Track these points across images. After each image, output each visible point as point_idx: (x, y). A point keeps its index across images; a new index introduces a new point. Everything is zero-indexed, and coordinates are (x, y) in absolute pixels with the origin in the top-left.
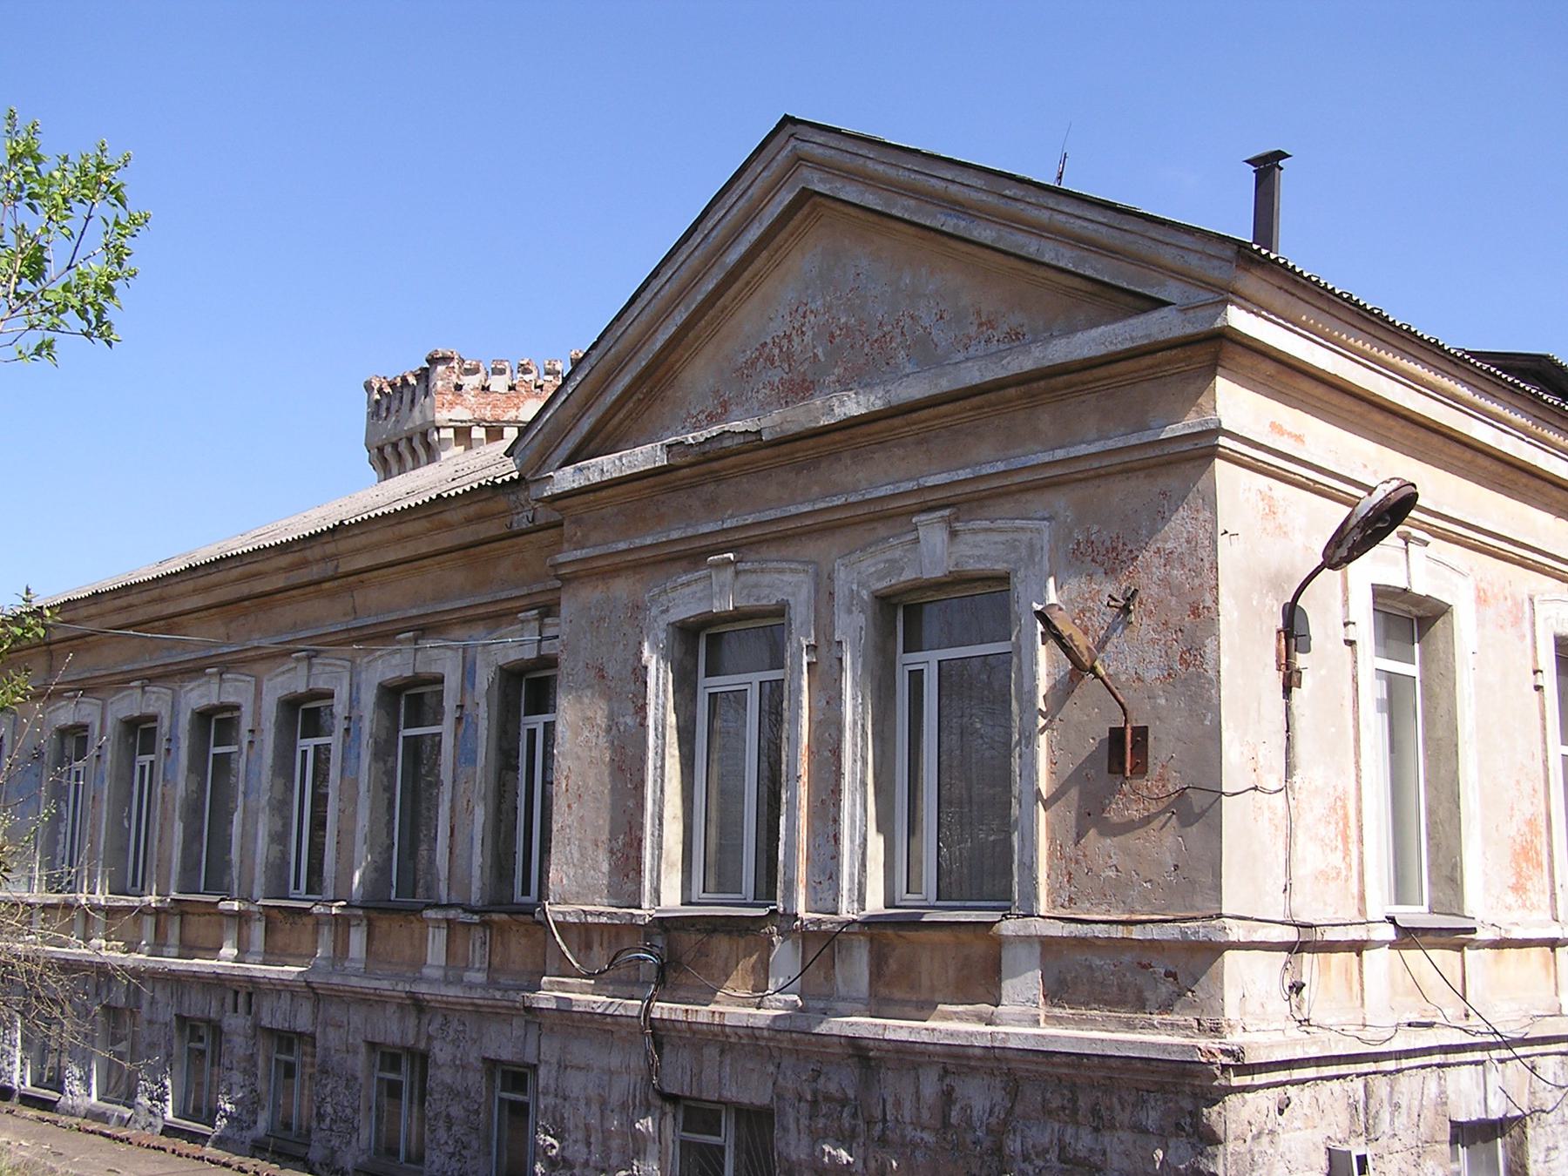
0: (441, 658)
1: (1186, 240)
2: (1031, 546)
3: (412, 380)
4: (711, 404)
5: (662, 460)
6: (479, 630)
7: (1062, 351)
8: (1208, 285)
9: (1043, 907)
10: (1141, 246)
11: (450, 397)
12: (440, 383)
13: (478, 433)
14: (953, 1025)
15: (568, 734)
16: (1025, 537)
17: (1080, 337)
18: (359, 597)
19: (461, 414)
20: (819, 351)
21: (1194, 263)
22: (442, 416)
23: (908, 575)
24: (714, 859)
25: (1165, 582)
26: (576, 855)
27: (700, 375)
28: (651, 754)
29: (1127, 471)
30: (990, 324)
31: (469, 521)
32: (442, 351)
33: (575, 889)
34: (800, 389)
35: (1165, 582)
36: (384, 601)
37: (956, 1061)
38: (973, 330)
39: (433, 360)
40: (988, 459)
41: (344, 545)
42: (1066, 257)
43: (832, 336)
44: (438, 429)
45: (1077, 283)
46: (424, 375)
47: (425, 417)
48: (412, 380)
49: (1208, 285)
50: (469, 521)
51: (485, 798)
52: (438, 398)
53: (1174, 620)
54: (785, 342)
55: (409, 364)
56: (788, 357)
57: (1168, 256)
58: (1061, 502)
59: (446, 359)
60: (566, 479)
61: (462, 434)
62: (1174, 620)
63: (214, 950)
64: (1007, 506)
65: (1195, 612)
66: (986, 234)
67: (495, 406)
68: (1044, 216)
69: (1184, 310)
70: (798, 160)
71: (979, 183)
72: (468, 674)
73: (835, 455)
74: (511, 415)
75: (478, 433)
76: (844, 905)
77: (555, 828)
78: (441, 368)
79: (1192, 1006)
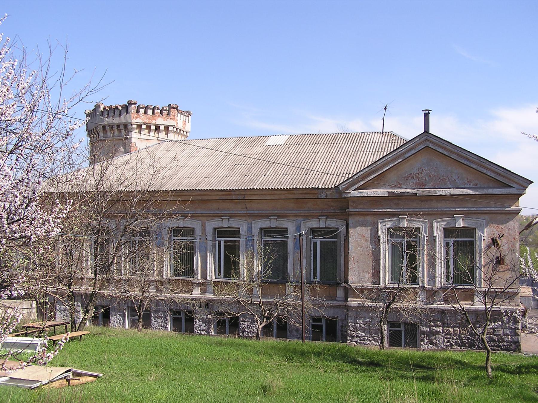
0: (290, 225)
1: (520, 178)
2: (481, 224)
3: (120, 108)
4: (396, 184)
5: (387, 195)
6: (300, 219)
7: (490, 191)
8: (523, 186)
9: (483, 286)
10: (511, 177)
12: (133, 111)
13: (144, 127)
14: (466, 305)
15: (353, 248)
16: (480, 222)
17: (495, 190)
18: (248, 205)
19: (139, 121)
20: (427, 178)
21: (521, 182)
22: (134, 121)
23: (452, 226)
24: (396, 276)
25: (508, 233)
26: (357, 274)
27: (392, 177)
28: (382, 254)
29: (502, 213)
30: (470, 181)
31: (301, 194)
32: (134, 101)
33: (357, 280)
34: (422, 185)
35: (508, 233)
36: (255, 207)
37: (464, 312)
38: (466, 182)
40: (470, 207)
41: (252, 193)
42: (493, 175)
43: (430, 176)
44: (132, 125)
45: (492, 179)
46: (126, 108)
48: (120, 108)
49: (523, 186)
50: (301, 194)
51: (306, 258)
52: (132, 115)
53: (510, 240)
54: (417, 175)
56: (418, 178)
57: (516, 180)
58: (486, 217)
59: (135, 104)
60: (356, 194)
61: (139, 126)
62: (510, 240)
63: (190, 291)
64: (474, 216)
65: (514, 239)
66: (475, 167)
68: (490, 167)
69: (517, 189)
70: (427, 140)
71: (475, 157)
72: (298, 229)
73: (432, 200)
74: (154, 122)
75: (144, 127)
76: (437, 285)
77: (350, 268)
78: (133, 106)
79: (513, 302)
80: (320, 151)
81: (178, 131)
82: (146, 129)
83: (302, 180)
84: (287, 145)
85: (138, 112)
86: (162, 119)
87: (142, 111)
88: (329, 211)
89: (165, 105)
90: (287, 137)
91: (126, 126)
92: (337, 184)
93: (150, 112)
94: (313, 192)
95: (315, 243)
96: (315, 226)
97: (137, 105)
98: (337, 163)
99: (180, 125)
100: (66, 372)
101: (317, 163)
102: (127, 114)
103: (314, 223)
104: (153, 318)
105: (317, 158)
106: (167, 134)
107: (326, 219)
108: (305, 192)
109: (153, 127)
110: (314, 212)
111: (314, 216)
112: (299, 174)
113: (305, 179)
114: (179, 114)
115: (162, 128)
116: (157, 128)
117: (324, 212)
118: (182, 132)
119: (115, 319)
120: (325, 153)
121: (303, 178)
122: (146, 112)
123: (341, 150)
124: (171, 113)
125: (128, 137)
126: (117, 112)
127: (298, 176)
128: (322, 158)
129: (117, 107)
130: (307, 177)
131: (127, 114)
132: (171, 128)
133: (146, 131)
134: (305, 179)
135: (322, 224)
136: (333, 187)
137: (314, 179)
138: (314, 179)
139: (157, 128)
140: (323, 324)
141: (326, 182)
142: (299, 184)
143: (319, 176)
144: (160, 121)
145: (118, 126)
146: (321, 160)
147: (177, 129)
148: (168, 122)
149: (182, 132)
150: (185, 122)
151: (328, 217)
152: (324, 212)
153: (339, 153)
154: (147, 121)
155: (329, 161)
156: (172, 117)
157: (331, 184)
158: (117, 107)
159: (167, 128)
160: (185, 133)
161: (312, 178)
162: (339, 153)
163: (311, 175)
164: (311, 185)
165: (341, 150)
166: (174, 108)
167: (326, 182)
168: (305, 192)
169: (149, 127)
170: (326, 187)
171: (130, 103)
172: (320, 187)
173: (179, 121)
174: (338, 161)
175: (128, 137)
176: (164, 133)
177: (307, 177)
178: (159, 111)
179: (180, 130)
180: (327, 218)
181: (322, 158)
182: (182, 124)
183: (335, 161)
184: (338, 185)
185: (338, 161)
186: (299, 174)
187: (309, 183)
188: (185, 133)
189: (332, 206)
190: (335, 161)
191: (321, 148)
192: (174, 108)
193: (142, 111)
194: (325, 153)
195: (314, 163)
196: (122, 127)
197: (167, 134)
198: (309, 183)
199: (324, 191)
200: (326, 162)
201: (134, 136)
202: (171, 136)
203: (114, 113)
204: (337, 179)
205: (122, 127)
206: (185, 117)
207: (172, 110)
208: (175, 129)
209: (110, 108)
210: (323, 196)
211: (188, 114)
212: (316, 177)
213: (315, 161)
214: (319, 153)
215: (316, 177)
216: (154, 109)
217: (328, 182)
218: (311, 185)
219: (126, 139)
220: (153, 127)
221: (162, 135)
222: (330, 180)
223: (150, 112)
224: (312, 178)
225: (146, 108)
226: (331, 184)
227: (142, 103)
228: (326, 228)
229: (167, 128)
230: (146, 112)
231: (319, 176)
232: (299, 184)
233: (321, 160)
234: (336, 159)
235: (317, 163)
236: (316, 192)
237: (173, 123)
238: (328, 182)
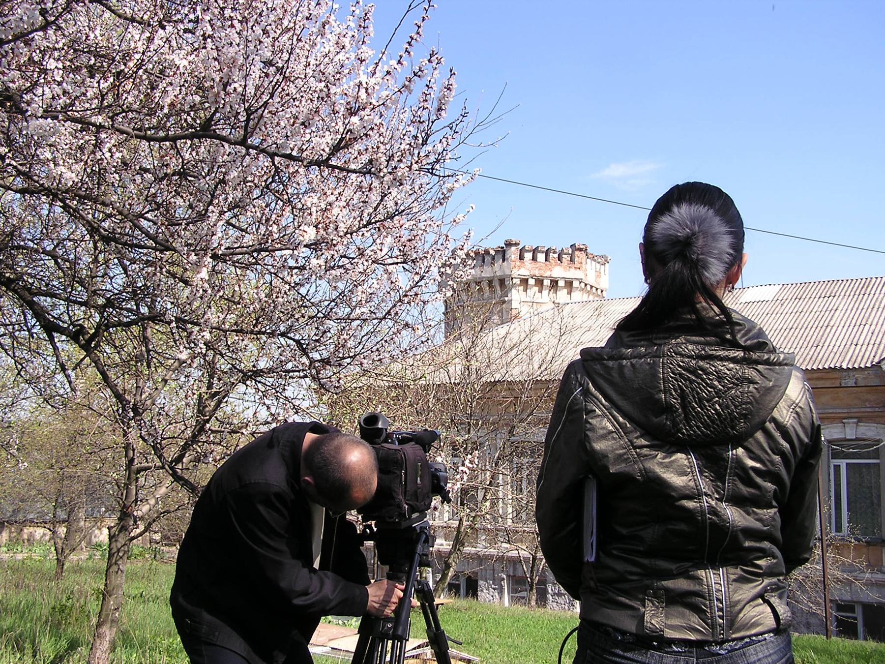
3: (492, 252)
11: (518, 263)
12: (513, 256)
13: (531, 282)
19: (524, 272)
22: (515, 273)
32: (514, 240)
39: (509, 244)
46: (502, 253)
47: (504, 271)
52: (513, 264)
55: (494, 243)
59: (516, 244)
61: (524, 282)
67: (540, 269)
74: (548, 274)
75: (531, 282)
78: (513, 248)
80: (840, 309)
81: (589, 287)
82: (536, 285)
83: (809, 356)
84: (778, 301)
85: (521, 258)
86: (562, 269)
87: (528, 256)
88: (863, 410)
89: (566, 246)
90: (778, 288)
91: (502, 282)
92: (876, 360)
93: (541, 257)
94: (831, 375)
95: (837, 468)
96: (837, 436)
97: (520, 247)
98: (873, 327)
99: (591, 280)
100: (419, 647)
101: (834, 328)
102: (503, 261)
103: (835, 430)
104: (549, 596)
105: (834, 319)
106: (570, 293)
107: (857, 423)
108: (816, 375)
109: (547, 282)
110: (834, 411)
111: (834, 418)
112: (805, 346)
113: (816, 354)
114: (589, 260)
115: (561, 283)
116: (554, 283)
117: (853, 410)
118: (594, 289)
119: (486, 594)
120: (849, 311)
121: (811, 353)
122: (534, 259)
123: (877, 304)
124: (576, 259)
125: (506, 299)
126: (488, 259)
127: (803, 350)
128: (845, 319)
129: (487, 252)
130: (818, 350)
131: (503, 261)
132: (576, 284)
133: (536, 289)
134: (816, 354)
135: (850, 433)
136: (869, 365)
137: (832, 355)
138: (832, 355)
139: (554, 283)
140: (859, 613)
141: (854, 358)
142: (806, 363)
143: (841, 349)
144: (559, 272)
145: (490, 282)
146: (843, 322)
147: (586, 285)
148: (571, 274)
149: (594, 289)
150: (598, 274)
151: (860, 420)
152: (853, 410)
153: (875, 309)
154: (537, 273)
155: (858, 324)
156: (577, 265)
157: (865, 360)
158: (487, 252)
159: (569, 284)
160: (599, 291)
161: (828, 352)
162: (875, 309)
163: (825, 348)
164: (828, 363)
165: (877, 304)
166: (581, 250)
167: (854, 358)
168: (816, 375)
169: (539, 282)
170: (856, 366)
171: (509, 244)
172: (844, 367)
173: (589, 271)
174: (875, 323)
175: (506, 299)
176: (565, 291)
177: (818, 350)
178: (556, 256)
179: (592, 287)
180: (859, 421)
181: (845, 319)
182: (594, 277)
183: (869, 322)
184: (879, 362)
185: (875, 323)
186: (805, 346)
187: (823, 361)
188: (599, 291)
189: (867, 400)
190: (869, 322)
191: (841, 303)
192: (581, 250)
193: (528, 256)
194: (849, 311)
195: (829, 328)
196: (496, 284)
197: (570, 293)
198: (823, 361)
199: (851, 374)
200: (852, 325)
201: (516, 296)
202: (577, 296)
203: (484, 261)
204: (876, 353)
205: (496, 284)
206: (598, 265)
207: (577, 253)
208: (583, 285)
209: (477, 253)
210: (851, 383)
211: (604, 260)
212: (835, 350)
213: (832, 323)
214: (838, 312)
215: (835, 350)
216: (547, 253)
217: (859, 358)
218: (828, 363)
219: (504, 302)
220: (547, 282)
221: (562, 295)
222: (861, 354)
223: (541, 257)
224: (828, 352)
225: (535, 251)
226: (865, 360)
227: (530, 244)
228: (857, 439)
229: (569, 284)
230: (534, 259)
231: (841, 349)
232: (806, 363)
233: (843, 322)
234: (870, 320)
235: (834, 328)
236: (837, 375)
237: (578, 274)
238: (859, 358)
